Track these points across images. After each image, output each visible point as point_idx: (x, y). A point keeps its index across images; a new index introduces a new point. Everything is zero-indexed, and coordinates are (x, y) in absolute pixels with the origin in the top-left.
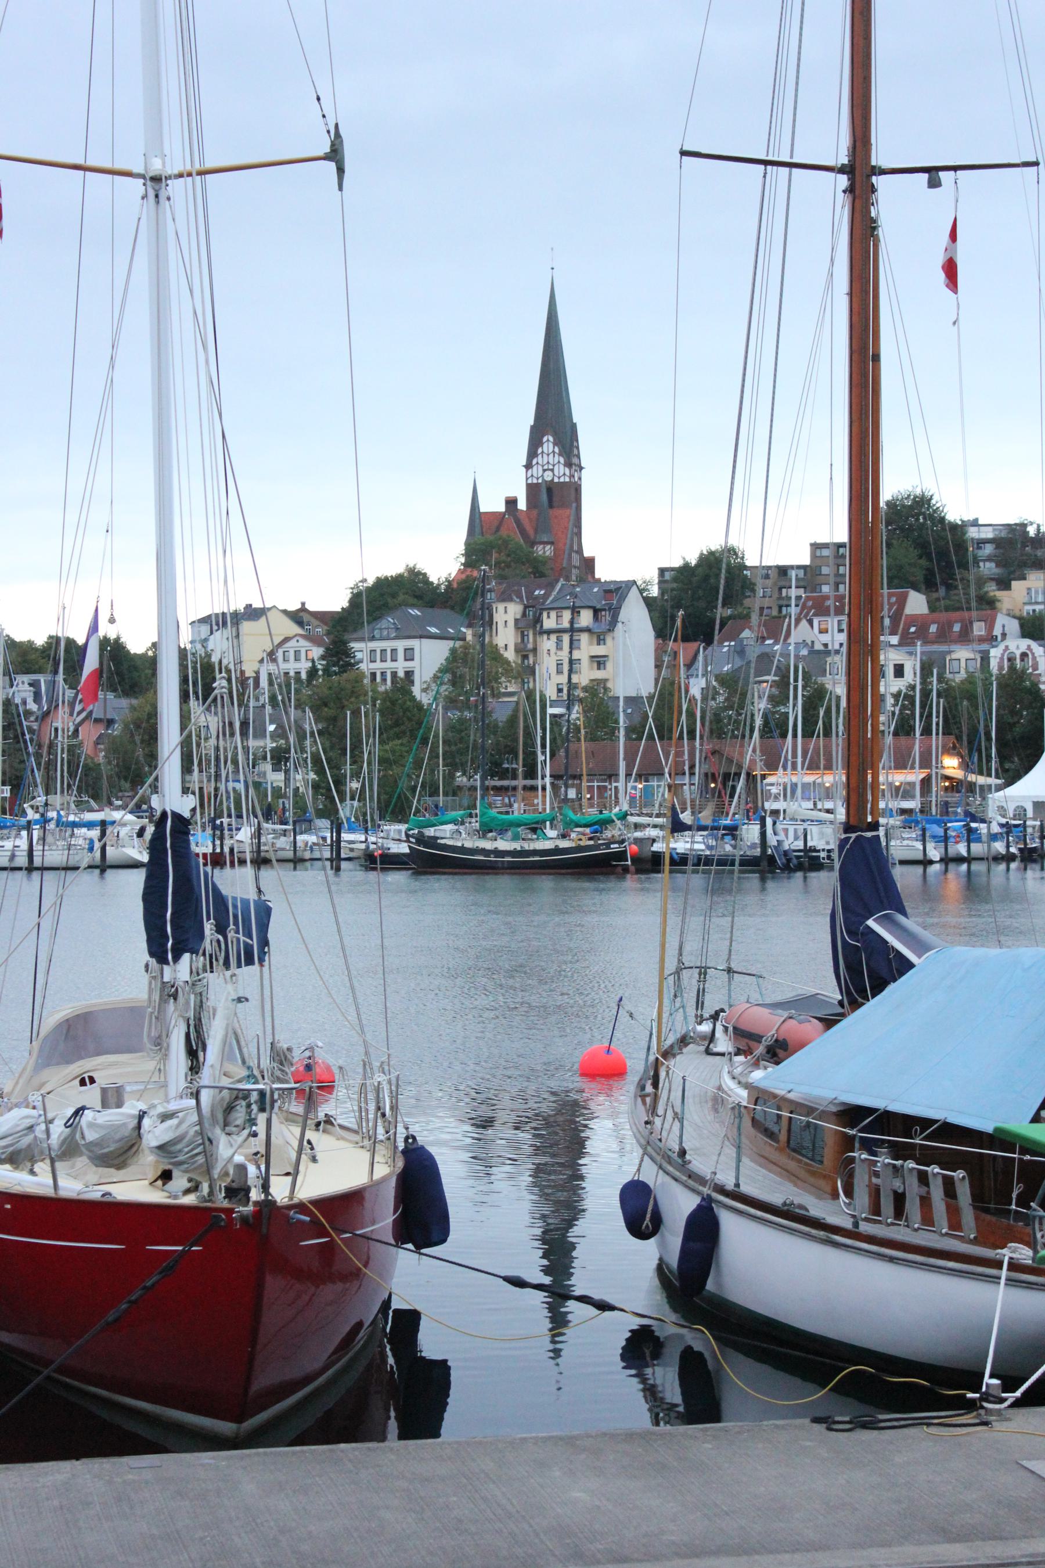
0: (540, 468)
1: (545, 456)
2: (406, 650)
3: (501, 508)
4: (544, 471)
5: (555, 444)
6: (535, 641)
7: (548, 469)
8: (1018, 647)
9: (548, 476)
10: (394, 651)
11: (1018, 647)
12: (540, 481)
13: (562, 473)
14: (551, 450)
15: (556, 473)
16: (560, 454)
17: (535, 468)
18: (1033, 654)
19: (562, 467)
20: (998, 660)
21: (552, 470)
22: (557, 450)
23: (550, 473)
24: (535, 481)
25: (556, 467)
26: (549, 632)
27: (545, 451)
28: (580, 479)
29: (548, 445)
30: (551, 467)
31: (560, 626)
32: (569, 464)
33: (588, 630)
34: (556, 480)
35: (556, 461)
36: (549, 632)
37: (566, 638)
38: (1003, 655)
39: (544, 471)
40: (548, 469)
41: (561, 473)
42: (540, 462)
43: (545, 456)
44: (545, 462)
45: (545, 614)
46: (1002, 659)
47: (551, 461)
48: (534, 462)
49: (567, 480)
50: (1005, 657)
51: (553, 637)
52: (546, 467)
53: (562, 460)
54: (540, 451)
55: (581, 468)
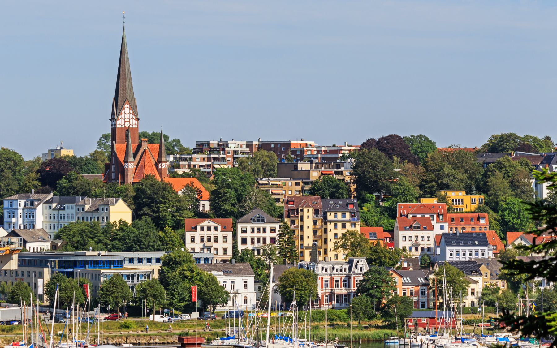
0: (123, 120)
4: (125, 122)
9: (127, 124)
12: (123, 126)
13: (134, 123)
14: (128, 112)
17: (120, 120)
19: (134, 120)
21: (129, 122)
22: (131, 112)
23: (128, 123)
24: (120, 126)
25: (131, 120)
26: (331, 222)
31: (336, 219)
33: (349, 221)
34: (131, 126)
35: (131, 117)
36: (331, 222)
39: (125, 122)
45: (328, 214)
53: (134, 117)
54: (123, 112)
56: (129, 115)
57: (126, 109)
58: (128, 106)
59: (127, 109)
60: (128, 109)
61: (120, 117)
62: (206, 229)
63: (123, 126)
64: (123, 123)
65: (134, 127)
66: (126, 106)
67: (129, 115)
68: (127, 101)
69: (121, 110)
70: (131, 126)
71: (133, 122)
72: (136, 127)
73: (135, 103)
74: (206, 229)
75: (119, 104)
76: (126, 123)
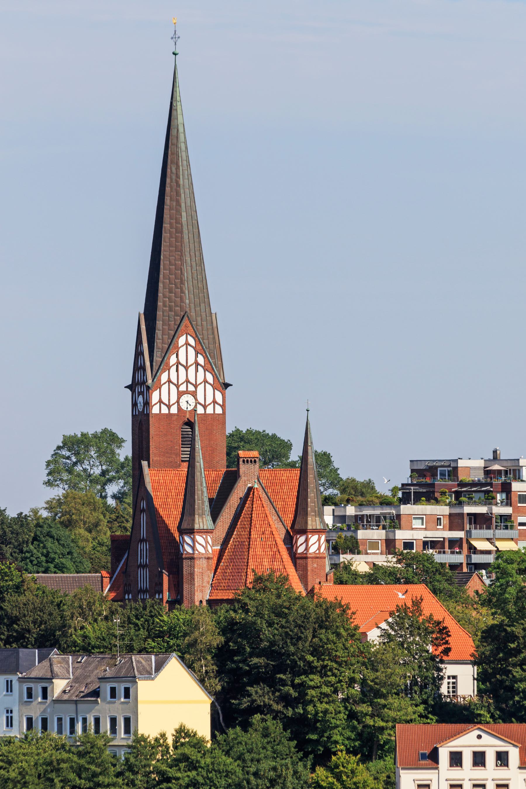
0: (173, 388)
4: (180, 394)
9: (187, 403)
12: (174, 410)
13: (209, 400)
14: (191, 360)
15: (201, 400)
19: (209, 388)
21: (194, 394)
22: (201, 360)
24: (165, 410)
25: (200, 389)
30: (191, 388)
34: (200, 410)
35: (200, 379)
40: (187, 392)
44: (182, 379)
52: (183, 388)
53: (210, 378)
54: (173, 360)
57: (182, 352)
58: (191, 341)
59: (186, 350)
60: (192, 352)
61: (164, 377)
62: (467, 759)
63: (174, 410)
64: (174, 399)
65: (210, 410)
66: (182, 341)
68: (186, 321)
69: (166, 353)
70: (200, 410)
71: (208, 394)
72: (219, 410)
73: (214, 331)
74: (467, 759)
75: (159, 333)
76: (184, 399)
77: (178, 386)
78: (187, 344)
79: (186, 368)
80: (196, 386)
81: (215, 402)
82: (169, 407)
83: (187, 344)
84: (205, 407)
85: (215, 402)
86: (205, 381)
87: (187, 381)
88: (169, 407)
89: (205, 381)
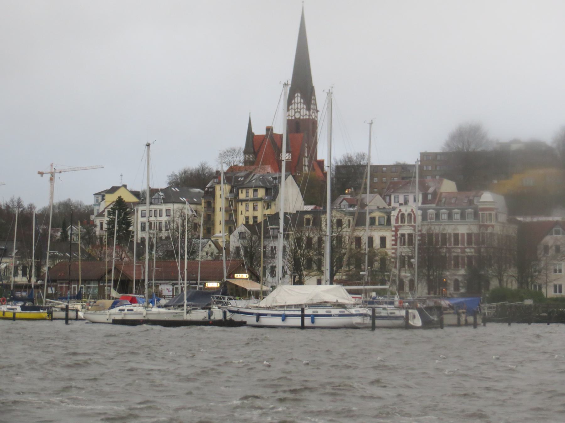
1: (296, 105)
2: (166, 210)
3: (264, 132)
4: (295, 112)
5: (301, 98)
6: (236, 206)
7: (297, 112)
8: (406, 211)
9: (297, 116)
10: (161, 211)
11: (406, 211)
12: (293, 118)
13: (305, 114)
14: (299, 101)
15: (302, 114)
16: (304, 103)
17: (291, 111)
18: (414, 214)
19: (305, 110)
20: (395, 217)
21: (300, 112)
22: (302, 101)
25: (302, 111)
27: (296, 101)
28: (316, 117)
29: (298, 98)
32: (308, 109)
34: (302, 118)
35: (302, 107)
37: (251, 205)
38: (398, 215)
40: (297, 112)
41: (304, 114)
42: (293, 108)
43: (296, 105)
46: (397, 217)
47: (299, 107)
48: (290, 107)
49: (308, 117)
50: (400, 215)
51: (244, 204)
53: (305, 107)
54: (293, 101)
55: (317, 111)
56: (299, 104)
57: (296, 99)
58: (299, 95)
59: (298, 98)
60: (299, 98)
63: (293, 118)
64: (293, 114)
65: (305, 117)
66: (296, 95)
67: (299, 104)
71: (304, 112)
76: (297, 114)
77: (295, 110)
78: (298, 96)
79: (298, 104)
80: (300, 110)
81: (306, 114)
82: (292, 117)
83: (298, 96)
84: (303, 116)
85: (306, 114)
86: (303, 108)
87: (298, 108)
88: (292, 117)
89: (303, 108)
